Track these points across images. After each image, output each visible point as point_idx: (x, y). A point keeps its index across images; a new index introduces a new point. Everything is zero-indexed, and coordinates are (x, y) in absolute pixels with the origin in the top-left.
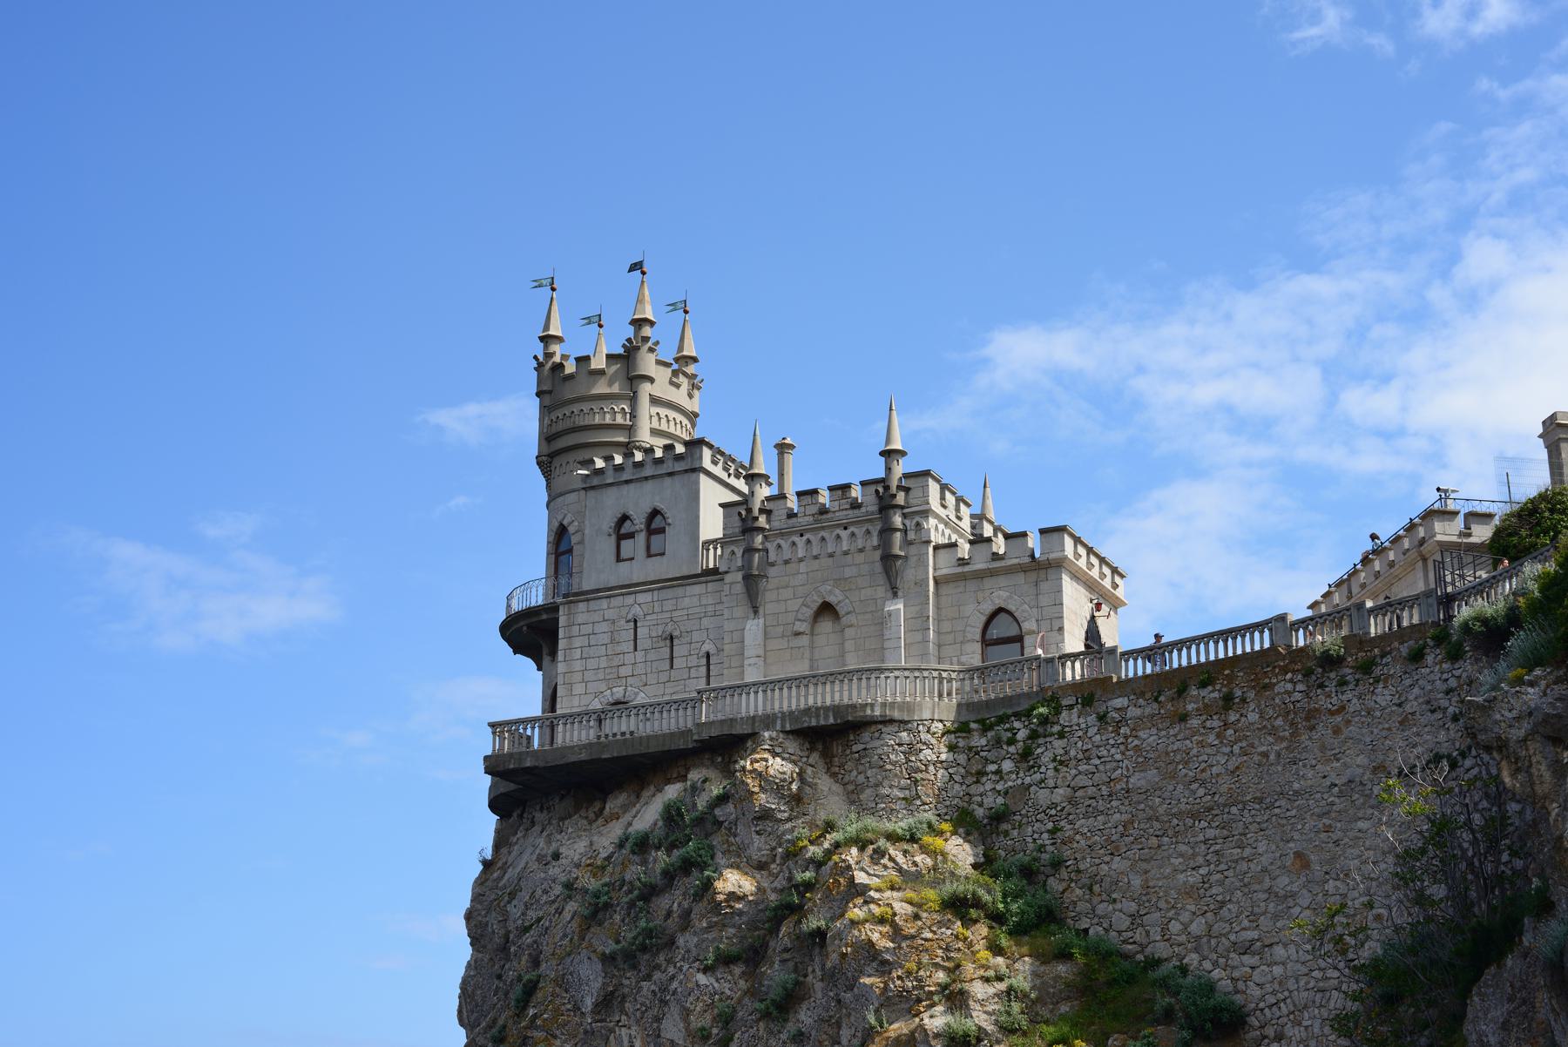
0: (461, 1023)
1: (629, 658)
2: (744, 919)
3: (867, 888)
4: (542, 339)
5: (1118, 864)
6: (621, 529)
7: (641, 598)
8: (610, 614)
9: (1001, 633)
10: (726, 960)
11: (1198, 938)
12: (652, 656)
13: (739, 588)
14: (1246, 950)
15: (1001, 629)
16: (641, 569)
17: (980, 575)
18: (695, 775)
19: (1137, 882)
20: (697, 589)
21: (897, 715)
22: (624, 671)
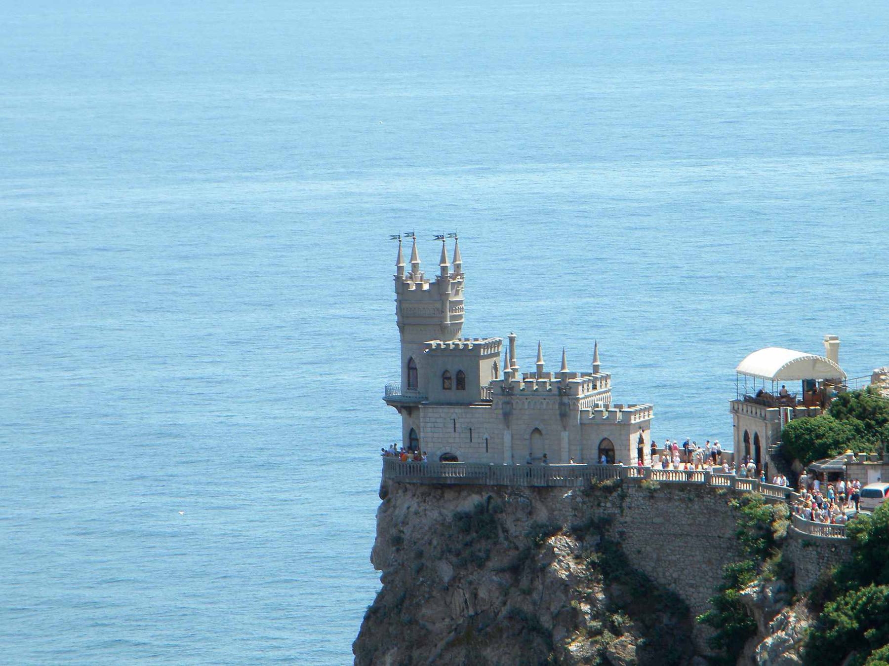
0: (372, 562)
1: (453, 435)
3: (559, 555)
5: (648, 548)
6: (445, 377)
7: (458, 410)
8: (443, 415)
10: (502, 571)
11: (675, 580)
12: (463, 435)
13: (501, 417)
14: (692, 586)
16: (454, 394)
17: (598, 425)
19: (655, 556)
22: (451, 440)
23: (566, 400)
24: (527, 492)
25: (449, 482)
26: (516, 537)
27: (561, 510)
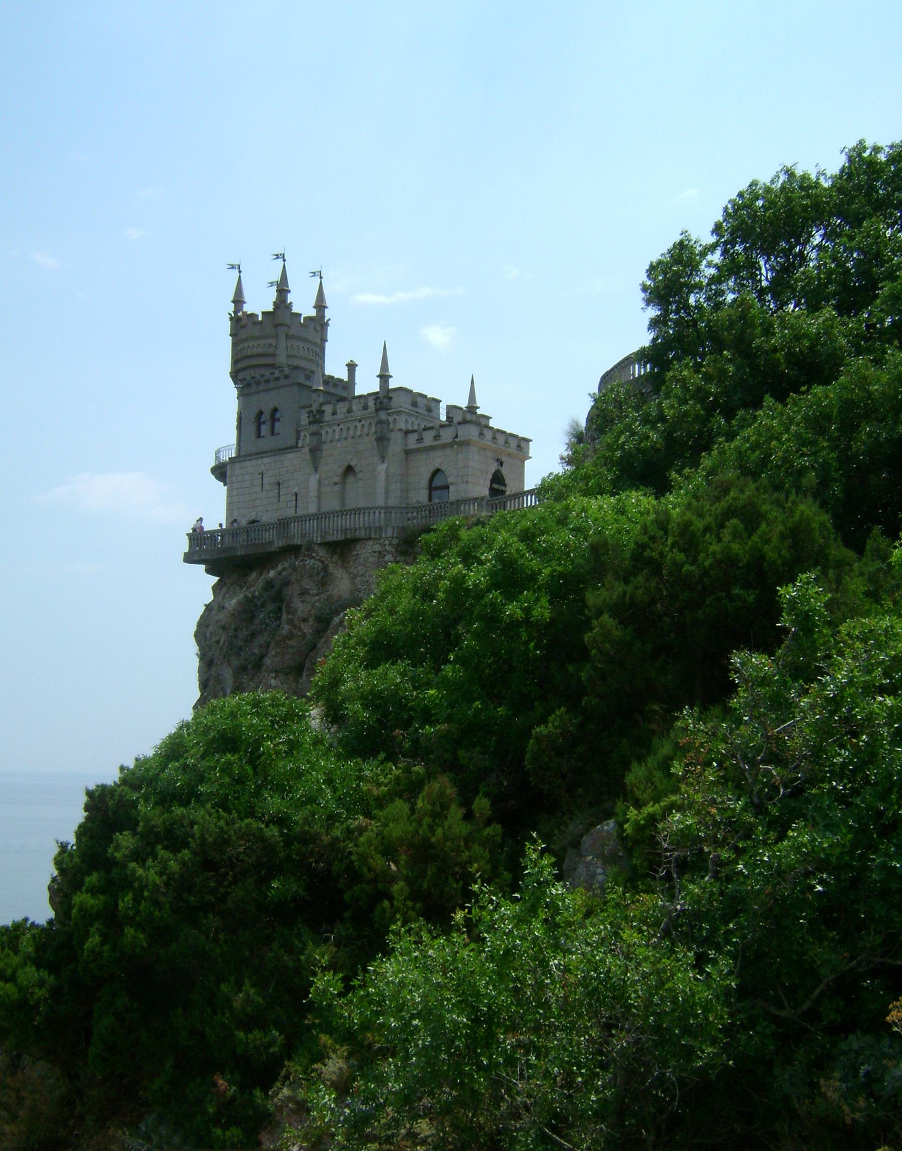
2: (294, 650)
4: (233, 302)
7: (266, 460)
9: (437, 483)
13: (308, 456)
15: (437, 482)
18: (280, 567)
20: (291, 456)
21: (373, 536)
22: (257, 503)
23: (383, 415)
24: (322, 552)
25: (239, 553)
26: (305, 620)
27: (362, 576)
